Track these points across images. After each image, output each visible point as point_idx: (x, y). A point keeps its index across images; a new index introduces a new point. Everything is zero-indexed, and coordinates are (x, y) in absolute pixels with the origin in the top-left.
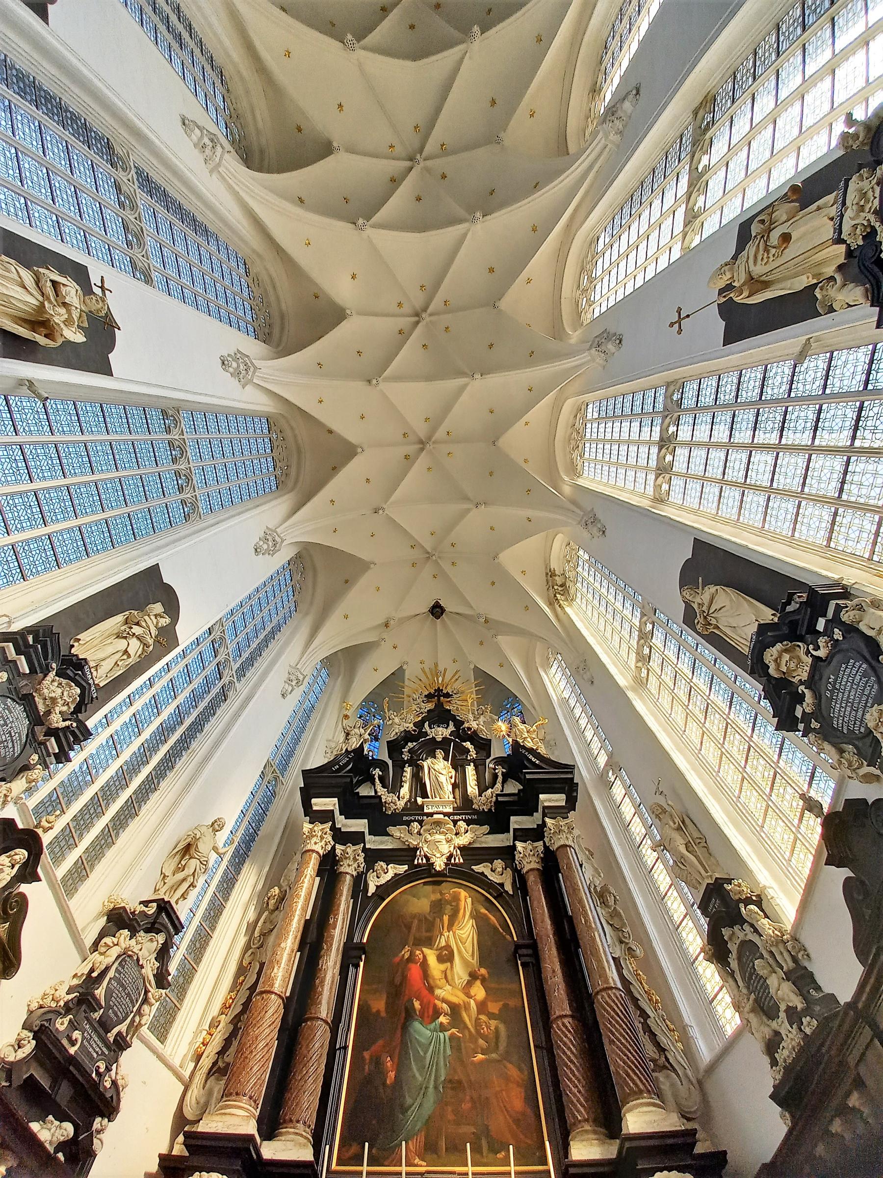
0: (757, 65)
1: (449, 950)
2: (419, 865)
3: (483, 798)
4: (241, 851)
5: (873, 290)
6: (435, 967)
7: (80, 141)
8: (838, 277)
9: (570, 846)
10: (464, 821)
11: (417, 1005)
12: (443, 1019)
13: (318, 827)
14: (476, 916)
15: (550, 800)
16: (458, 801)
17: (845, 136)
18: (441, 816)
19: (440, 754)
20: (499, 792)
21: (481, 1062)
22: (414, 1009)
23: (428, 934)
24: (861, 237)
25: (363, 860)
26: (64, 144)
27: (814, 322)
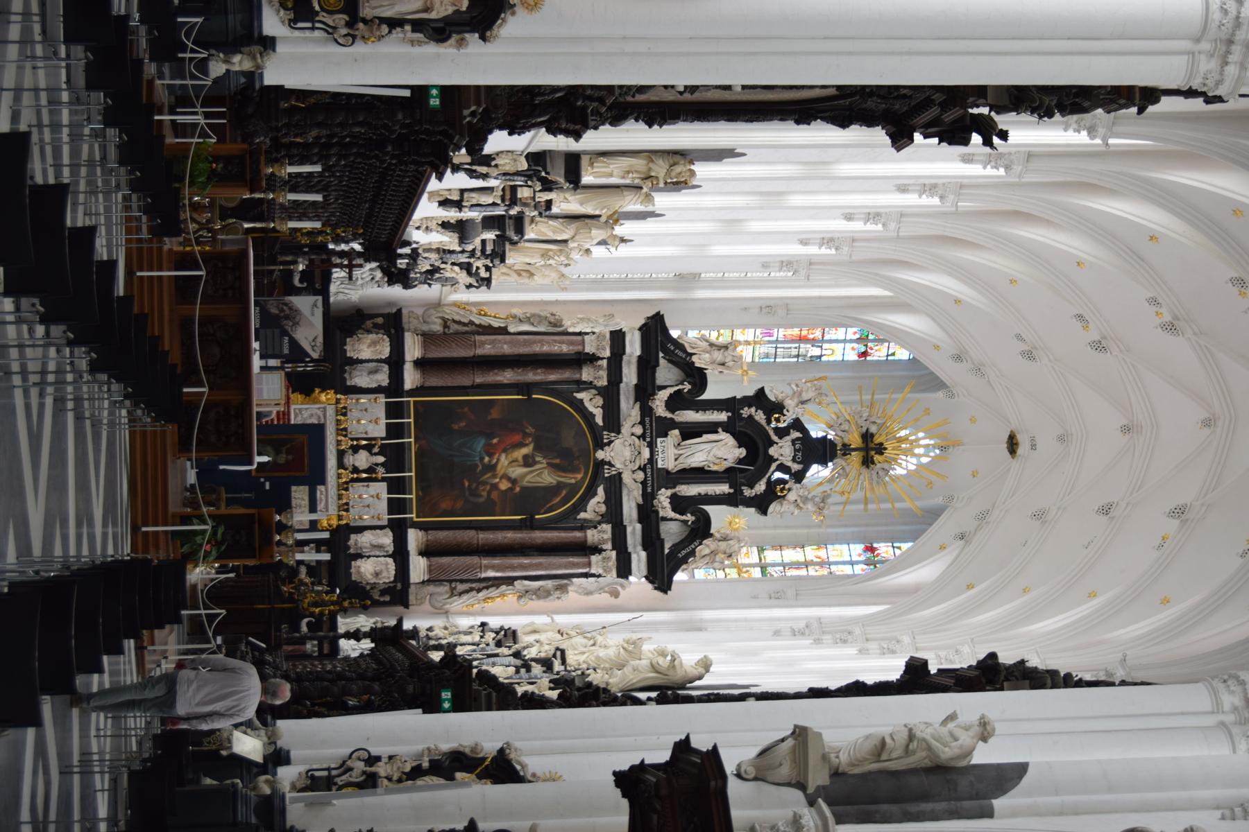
11: (495, 441)
12: (487, 459)
19: (742, 452)
21: (463, 484)
22: (494, 438)
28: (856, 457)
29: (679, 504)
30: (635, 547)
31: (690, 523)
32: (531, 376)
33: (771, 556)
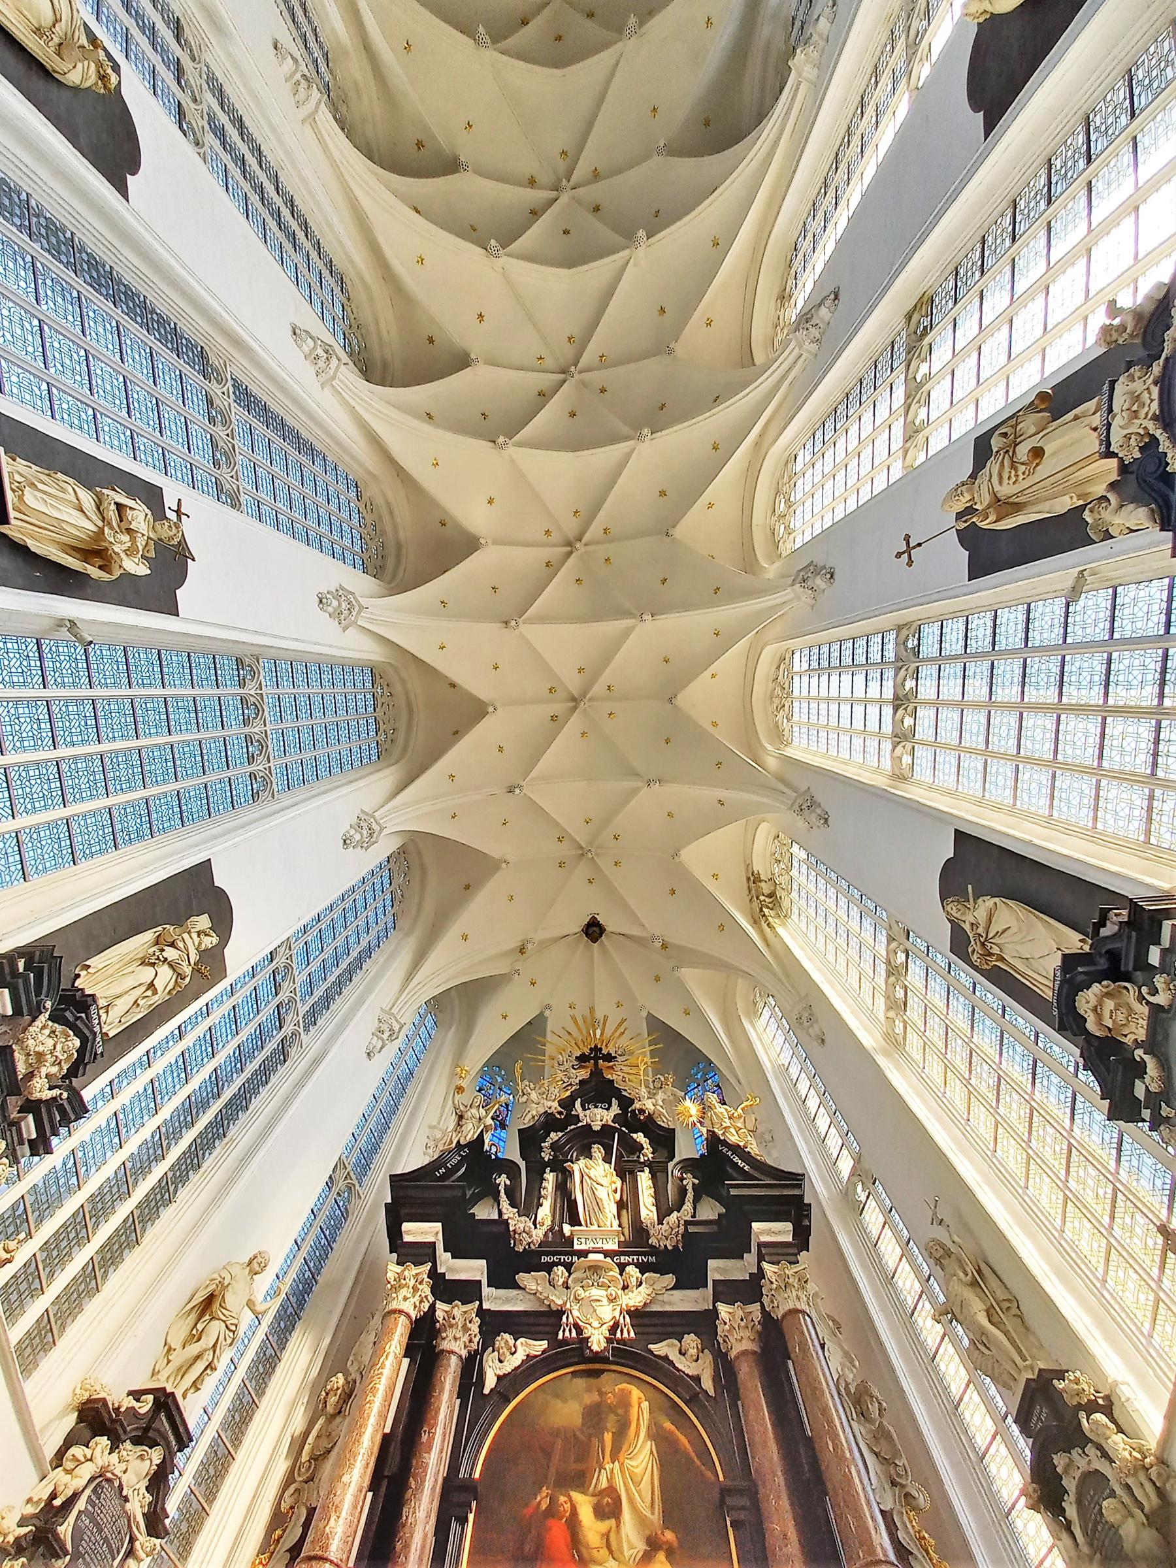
0: (1054, 181)
1: (614, 1495)
2: (565, 1342)
3: (665, 1227)
4: (290, 1310)
5: (1161, 511)
6: (591, 1527)
7: (168, 348)
8: (1112, 497)
9: (803, 1312)
13: (411, 1271)
14: (658, 1436)
15: (769, 1232)
16: (626, 1231)
17: (1106, 330)
18: (600, 1257)
19: (598, 1151)
20: (689, 1218)
23: (579, 1467)
24: (1137, 448)
25: (477, 1330)
26: (148, 350)
27: (1087, 550)
31: (696, 1181)
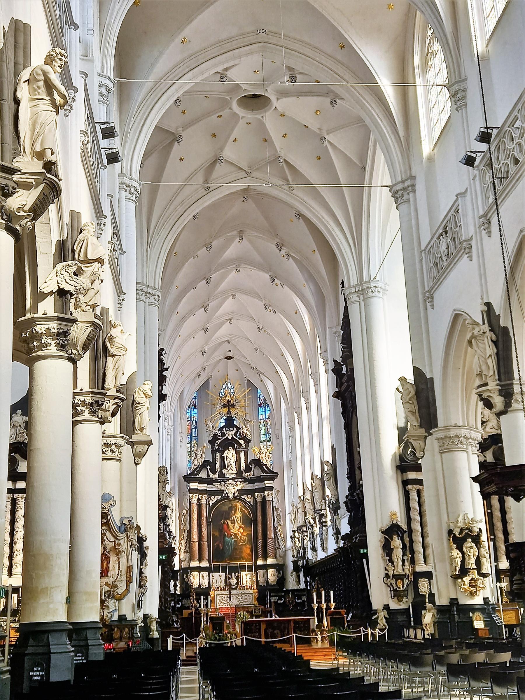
10: (240, 481)
12: (232, 537)
14: (242, 511)
28: (231, 410)
29: (248, 469)
30: (263, 485)
32: (204, 522)
33: (263, 438)
